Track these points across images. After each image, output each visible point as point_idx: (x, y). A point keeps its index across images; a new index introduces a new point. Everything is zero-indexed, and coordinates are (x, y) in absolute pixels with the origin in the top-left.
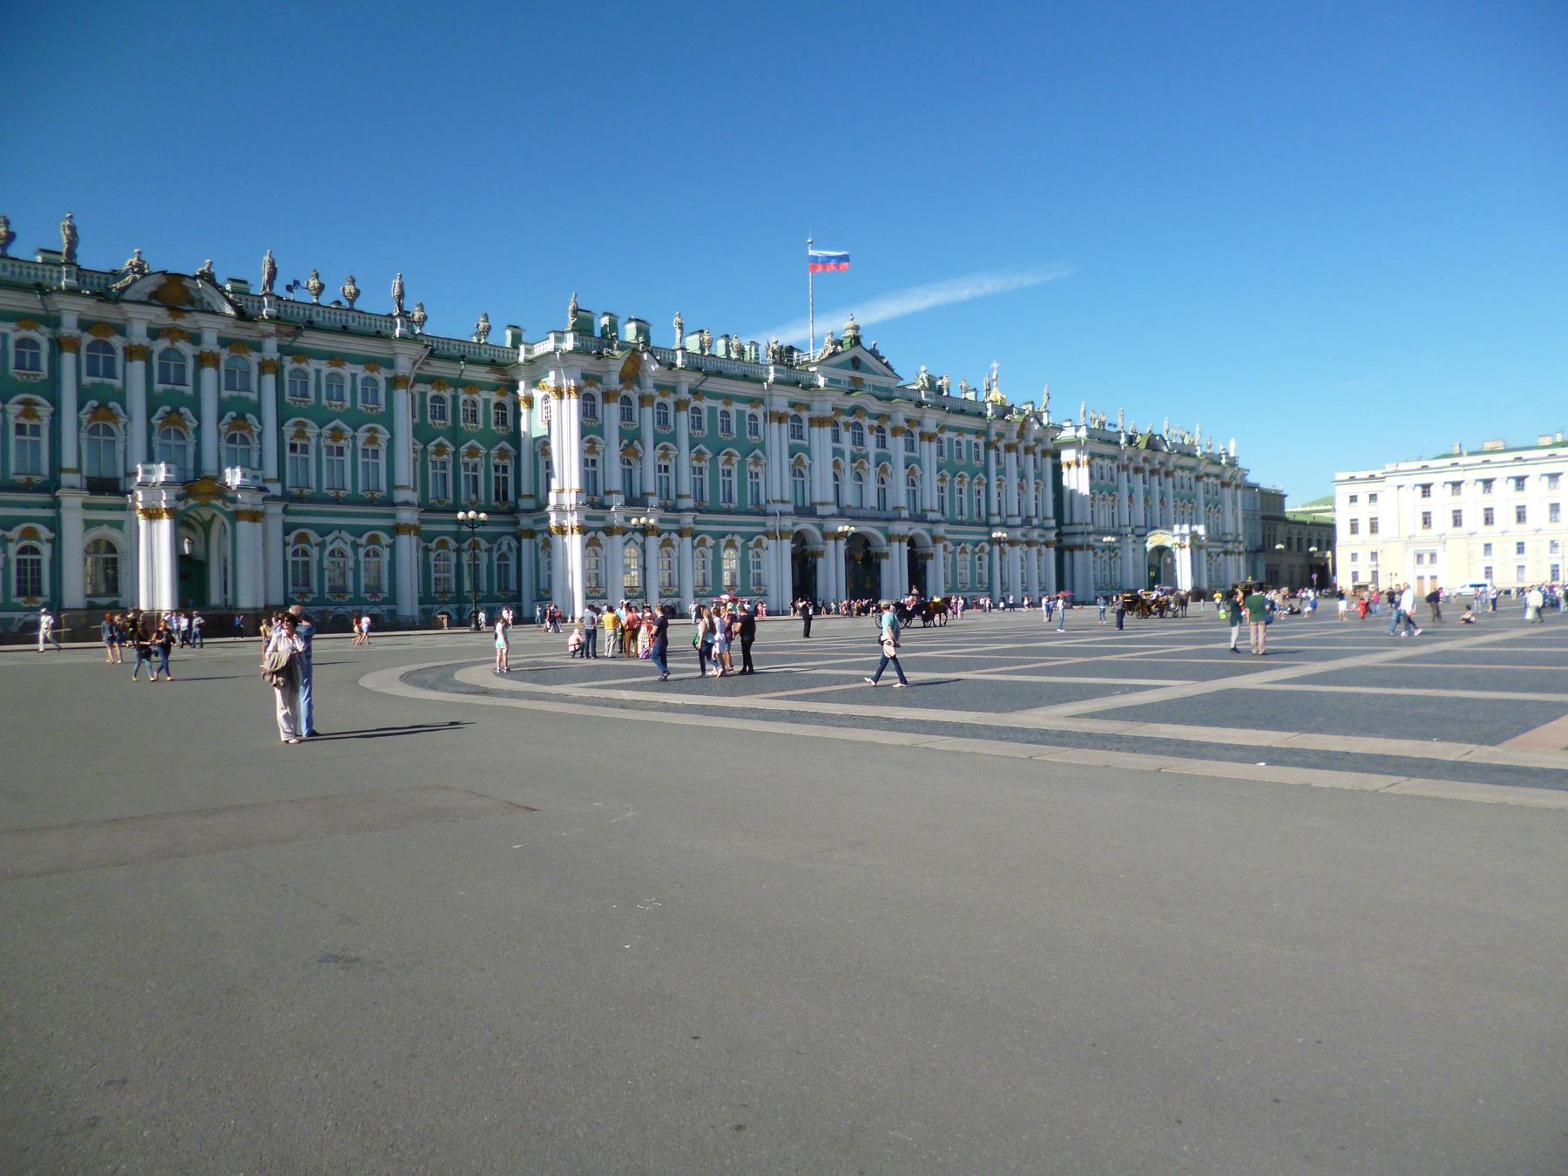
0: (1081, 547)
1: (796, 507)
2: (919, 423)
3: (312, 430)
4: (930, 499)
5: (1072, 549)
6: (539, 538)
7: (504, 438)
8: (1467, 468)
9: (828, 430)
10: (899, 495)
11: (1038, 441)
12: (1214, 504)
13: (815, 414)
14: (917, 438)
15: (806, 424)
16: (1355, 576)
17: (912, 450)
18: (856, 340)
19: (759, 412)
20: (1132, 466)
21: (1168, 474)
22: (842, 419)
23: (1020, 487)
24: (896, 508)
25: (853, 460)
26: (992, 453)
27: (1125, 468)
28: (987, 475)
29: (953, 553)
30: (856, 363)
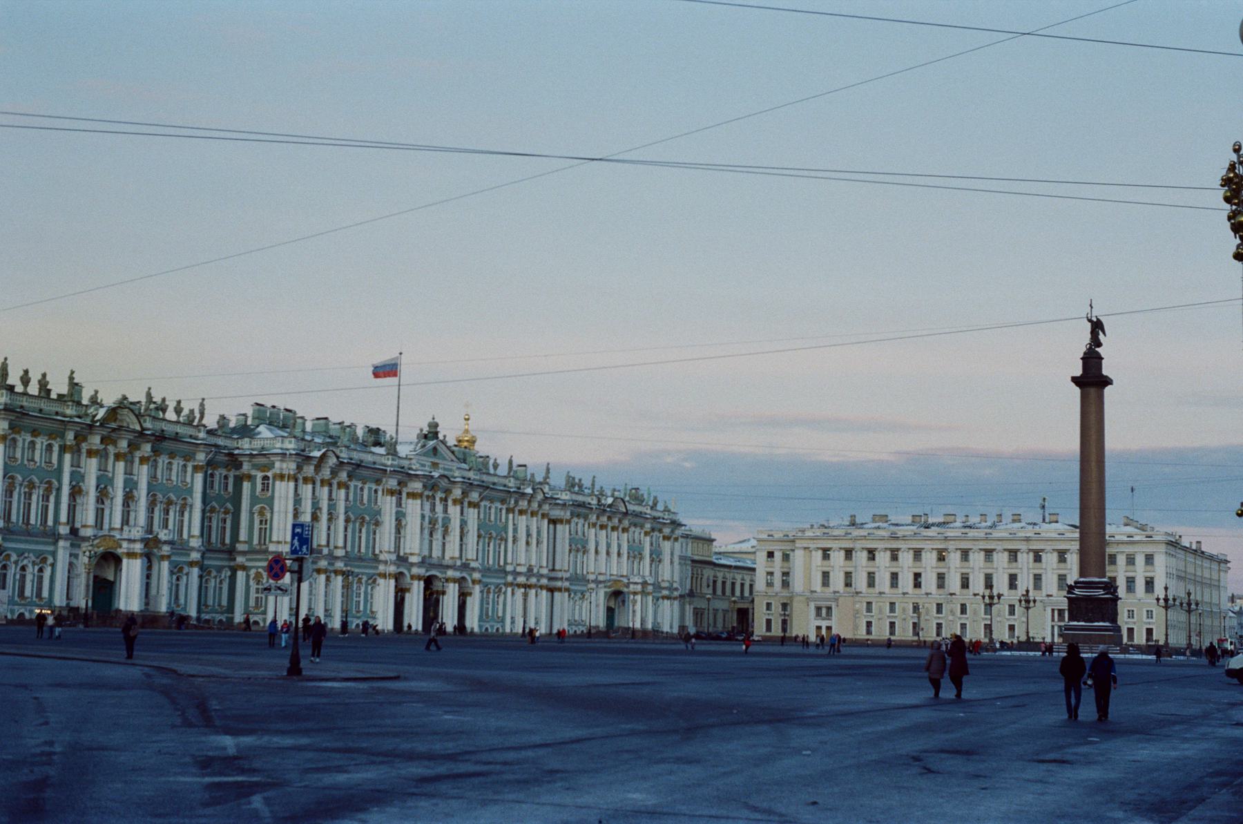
0: (560, 590)
1: (398, 556)
3: (160, 497)
4: (471, 554)
6: (253, 572)
7: (227, 500)
9: (419, 502)
10: (453, 550)
16: (769, 622)
19: (380, 488)
21: (624, 530)
22: (426, 493)
23: (528, 543)
24: (452, 558)
26: (511, 516)
27: (594, 525)
28: (506, 533)
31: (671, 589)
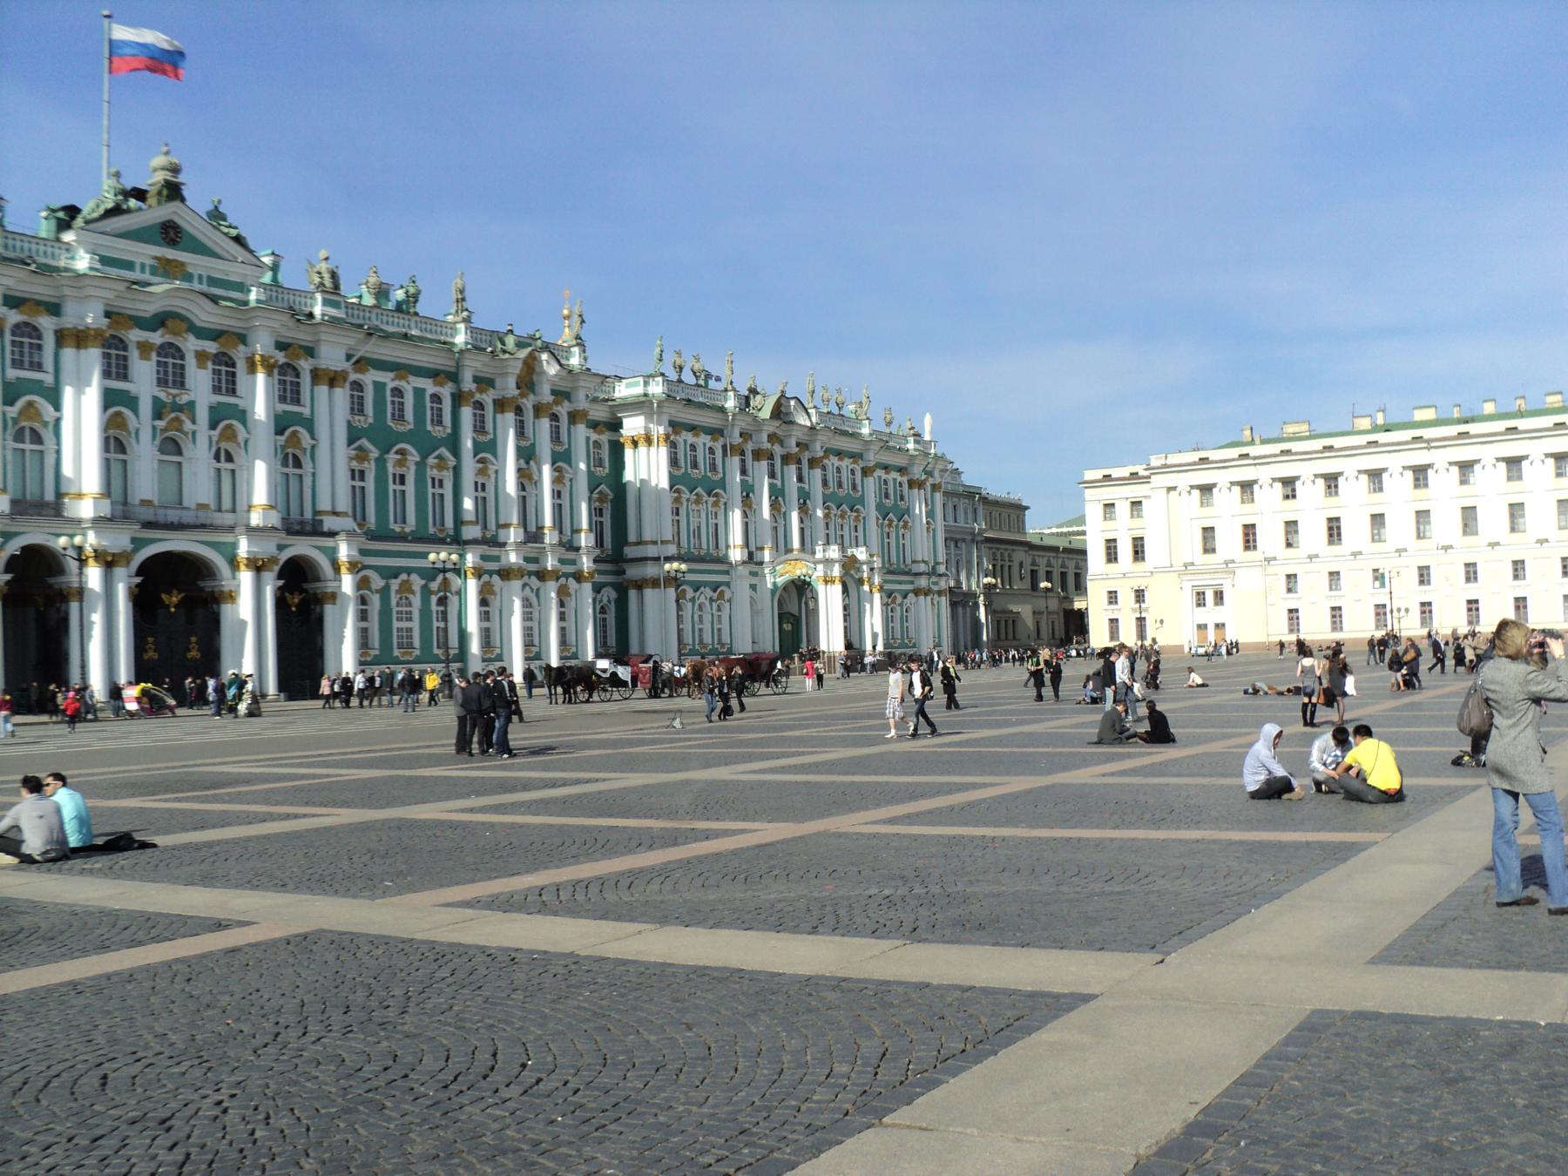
0: (655, 583)
2: (310, 352)
5: (640, 585)
8: (1261, 460)
11: (560, 395)
12: (894, 513)
13: (69, 321)
14: (306, 380)
15: (49, 342)
16: (1114, 622)
17: (297, 401)
18: (173, 191)
20: (749, 447)
21: (813, 463)
22: (135, 335)
25: (158, 415)
26: (467, 413)
28: (456, 450)
29: (384, 593)
30: (170, 233)
31: (933, 573)
